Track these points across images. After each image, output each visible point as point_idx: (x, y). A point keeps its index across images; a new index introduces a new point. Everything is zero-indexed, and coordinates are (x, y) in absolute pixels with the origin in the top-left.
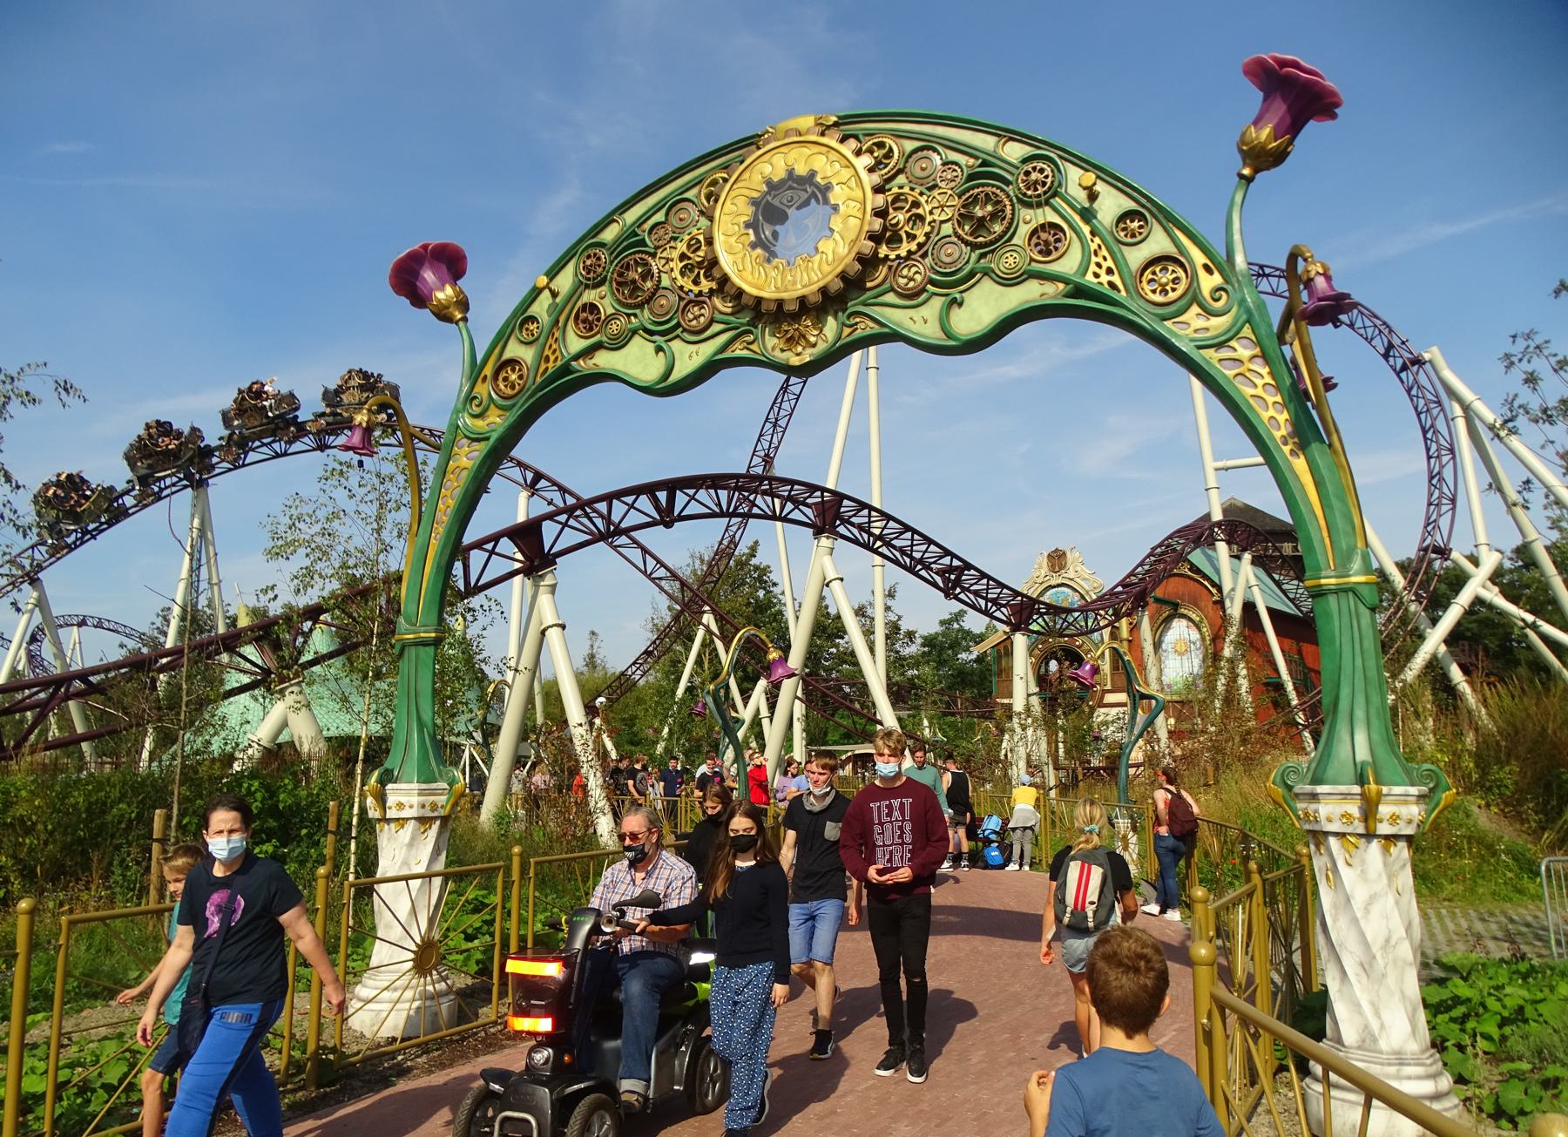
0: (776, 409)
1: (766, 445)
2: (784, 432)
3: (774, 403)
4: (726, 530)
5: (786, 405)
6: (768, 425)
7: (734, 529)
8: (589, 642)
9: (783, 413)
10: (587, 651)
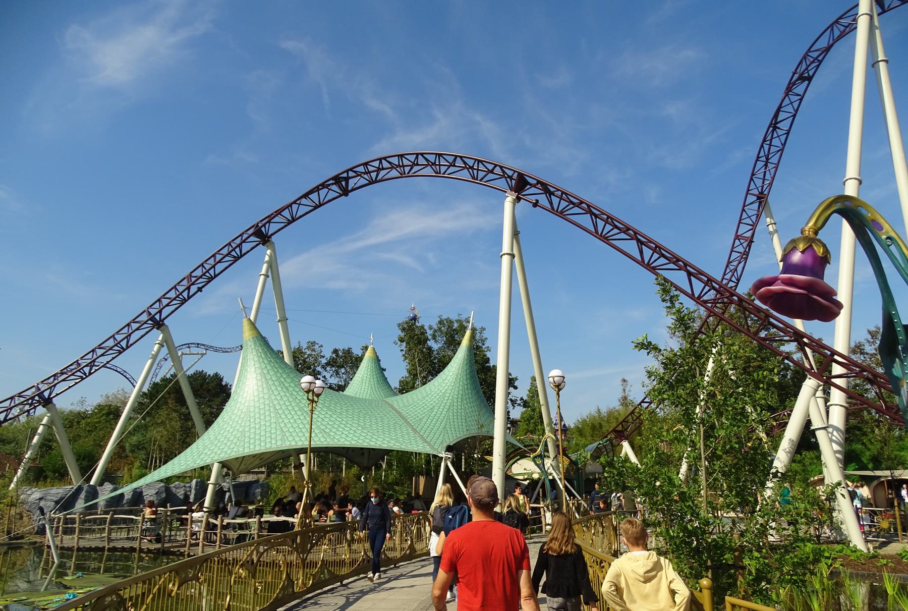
0: (766, 147)
1: (759, 183)
2: (777, 168)
3: (764, 140)
4: (727, 266)
5: (776, 142)
6: (760, 164)
7: (735, 263)
8: (622, 388)
9: (773, 149)
10: (620, 394)
